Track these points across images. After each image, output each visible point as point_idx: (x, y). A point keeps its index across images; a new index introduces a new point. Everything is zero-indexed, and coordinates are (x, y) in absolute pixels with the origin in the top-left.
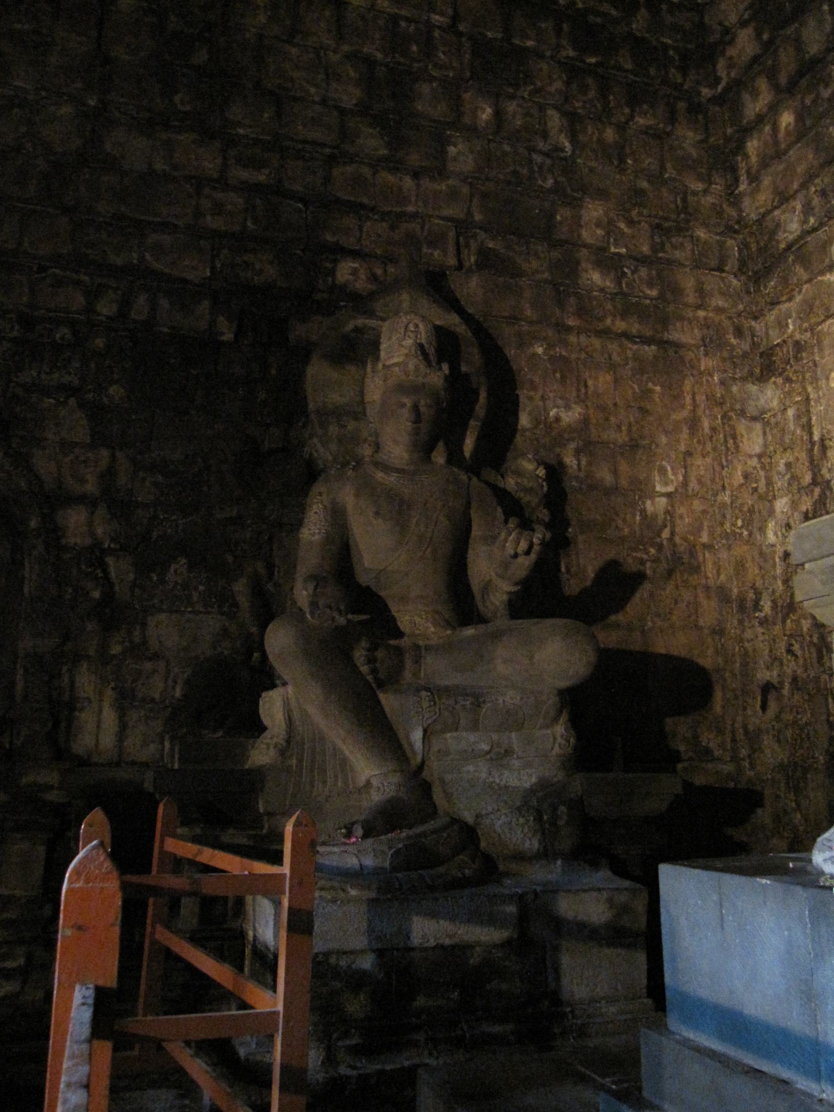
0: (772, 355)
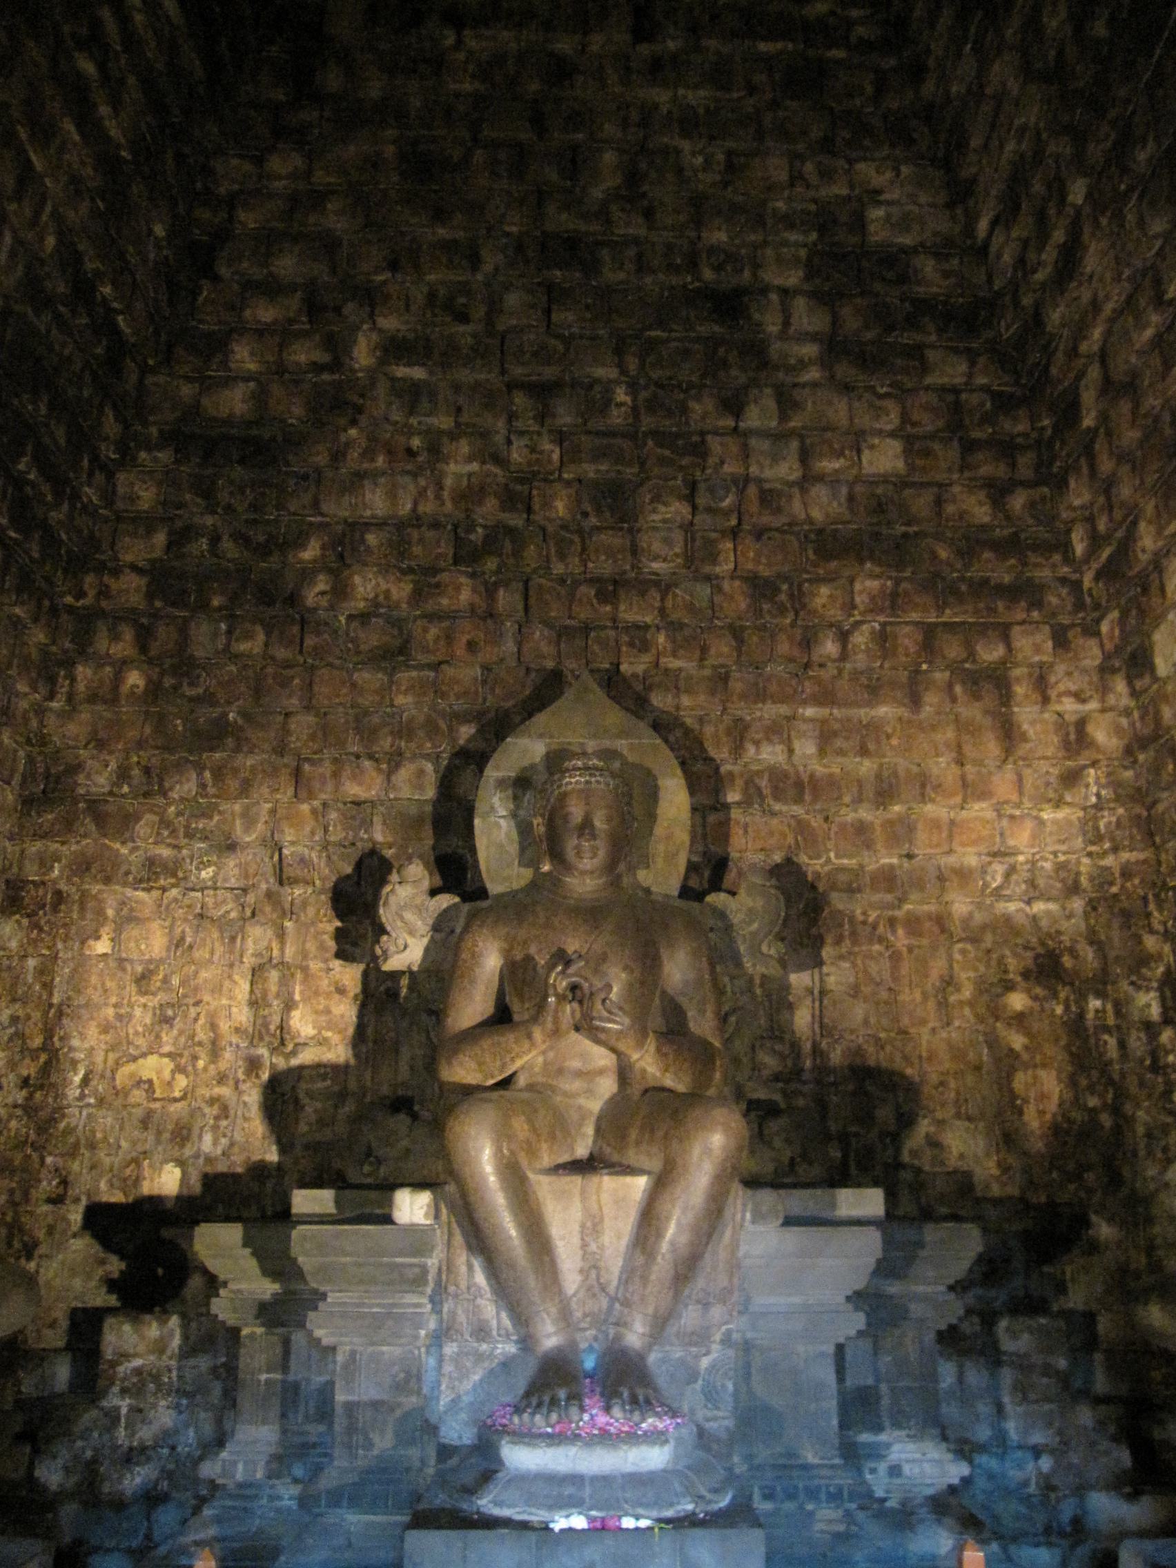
0: (22, 889)
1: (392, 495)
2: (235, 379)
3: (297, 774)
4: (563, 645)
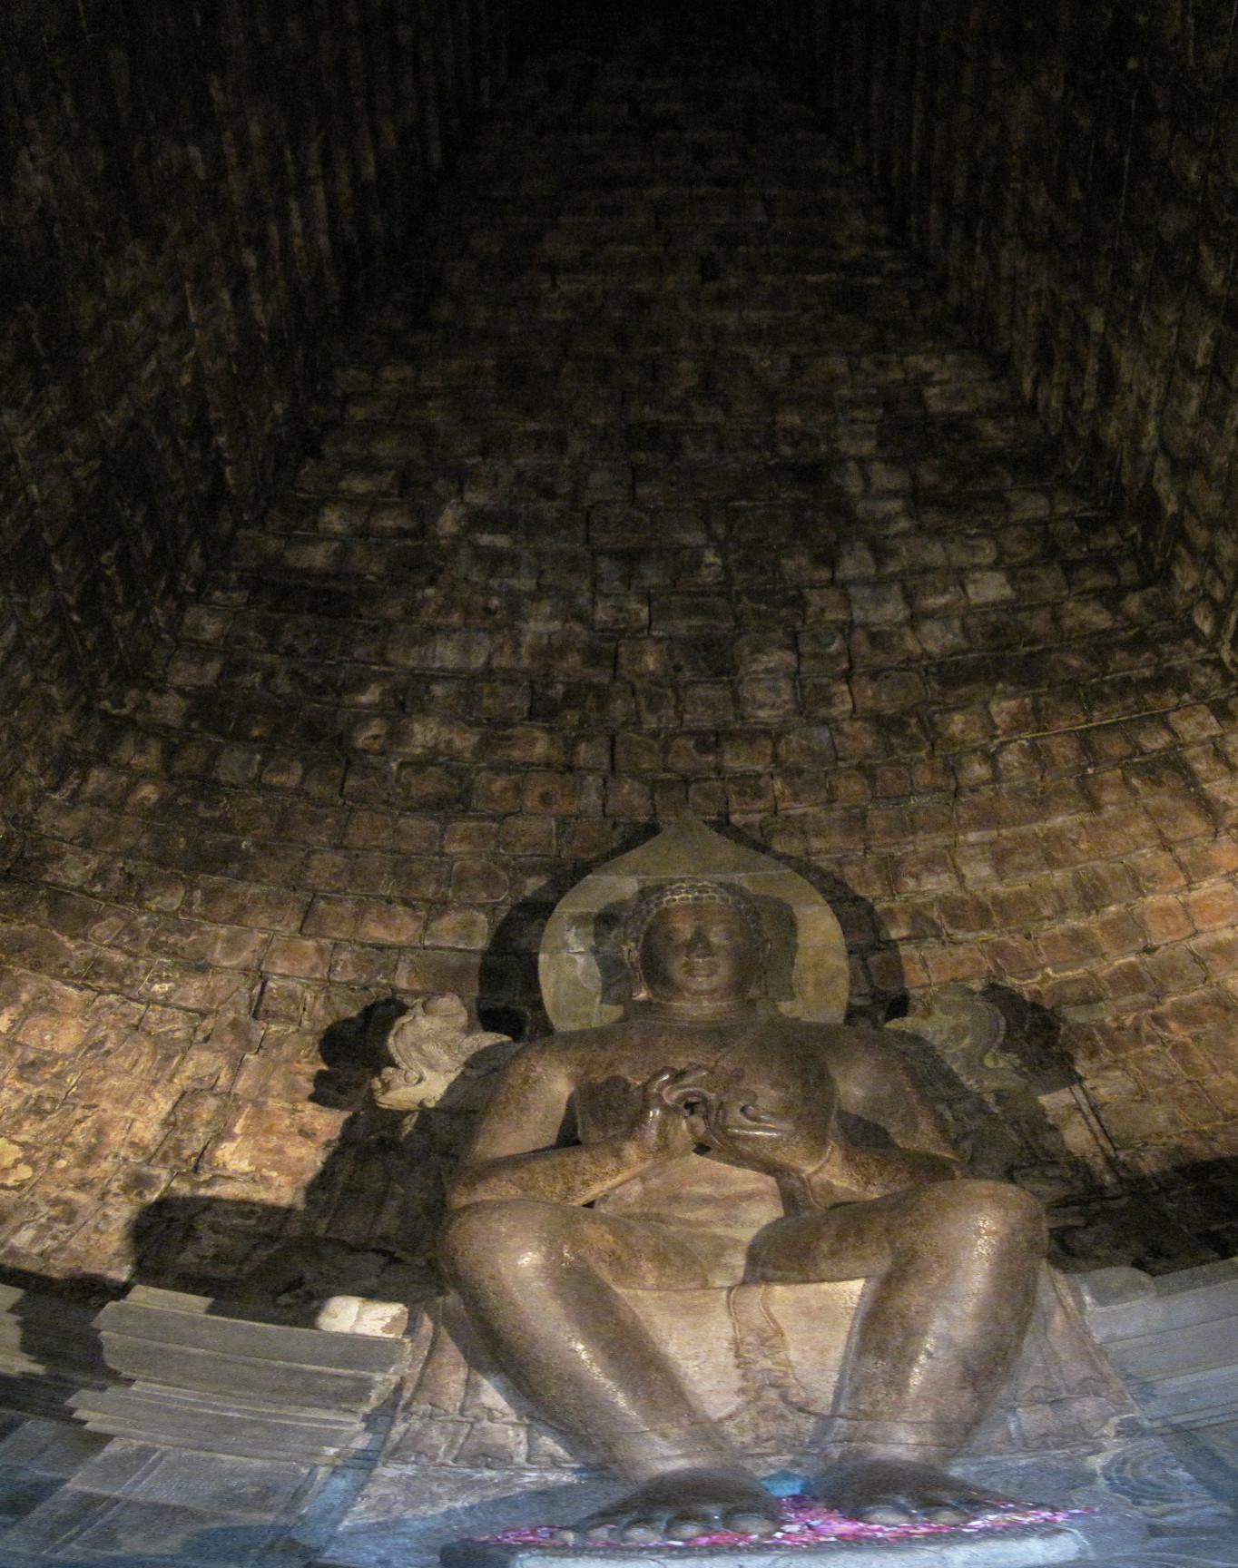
1: (465, 650)
2: (322, 540)
3: (308, 912)
4: (657, 798)
